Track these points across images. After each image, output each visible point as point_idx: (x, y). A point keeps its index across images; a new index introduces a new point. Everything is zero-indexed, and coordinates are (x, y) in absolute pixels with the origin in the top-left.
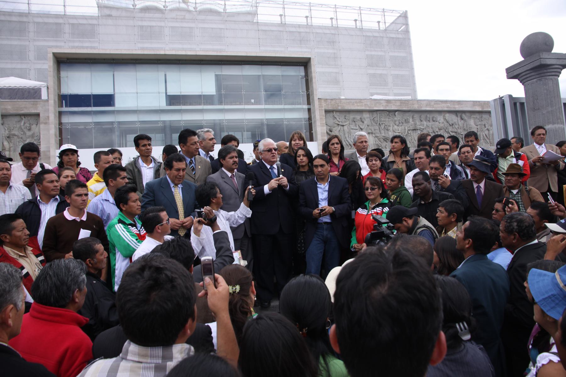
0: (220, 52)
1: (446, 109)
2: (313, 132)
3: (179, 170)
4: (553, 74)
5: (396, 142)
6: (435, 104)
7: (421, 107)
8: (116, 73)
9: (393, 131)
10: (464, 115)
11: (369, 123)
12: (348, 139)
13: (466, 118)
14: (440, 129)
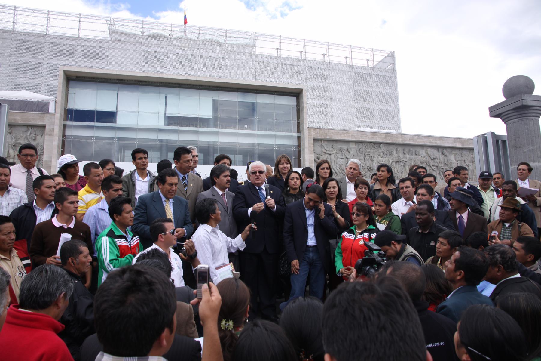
0: (219, 79)
1: (428, 144)
2: (302, 158)
3: (171, 184)
4: (534, 114)
5: (383, 171)
6: (418, 139)
7: (405, 141)
8: (120, 93)
9: (378, 162)
10: (445, 151)
11: (355, 154)
13: (447, 153)
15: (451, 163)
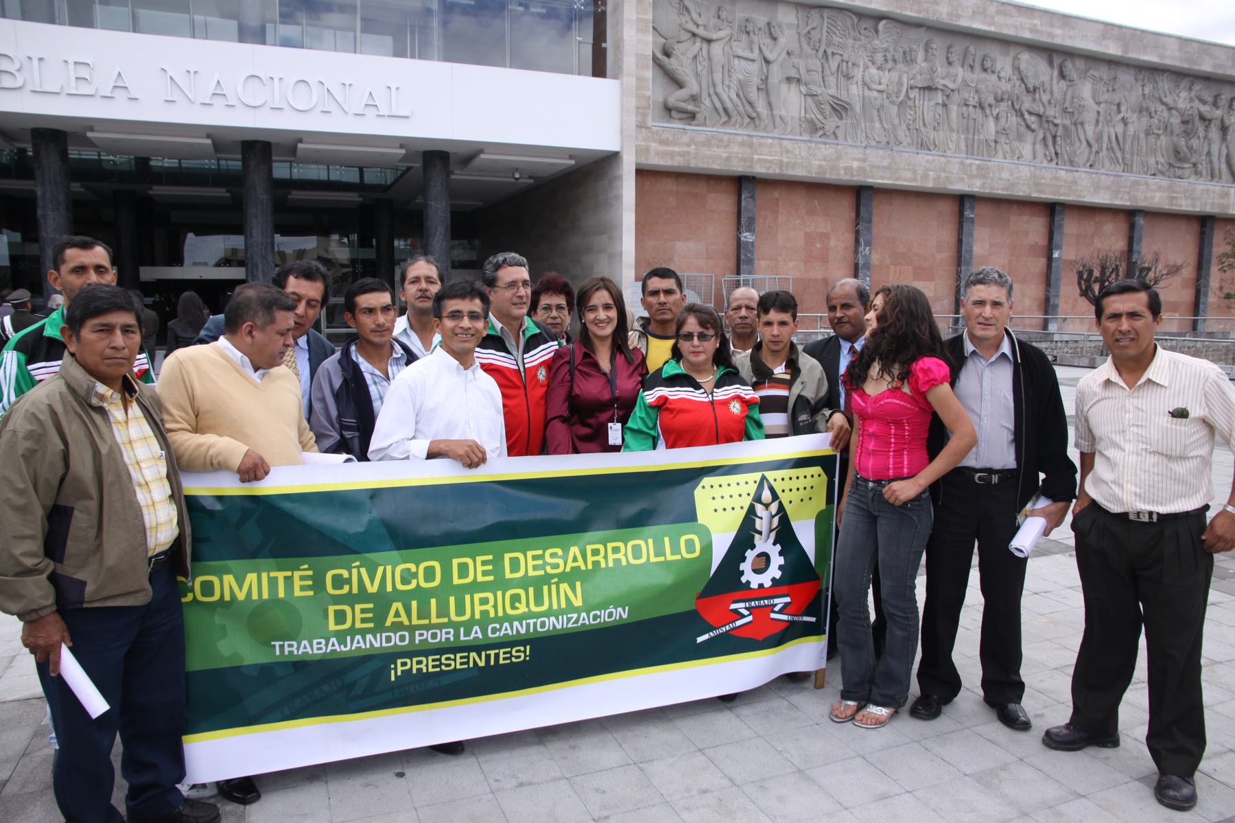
1: (1027, 35)
2: (609, 45)
6: (998, 12)
7: (959, 17)
9: (865, 84)
10: (1069, 64)
11: (794, 47)
12: (720, 89)
13: (1074, 76)
14: (999, 100)
15: (1082, 107)
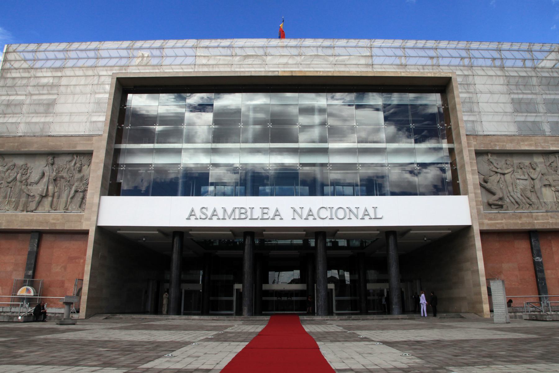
2: (460, 181)
12: (512, 194)
